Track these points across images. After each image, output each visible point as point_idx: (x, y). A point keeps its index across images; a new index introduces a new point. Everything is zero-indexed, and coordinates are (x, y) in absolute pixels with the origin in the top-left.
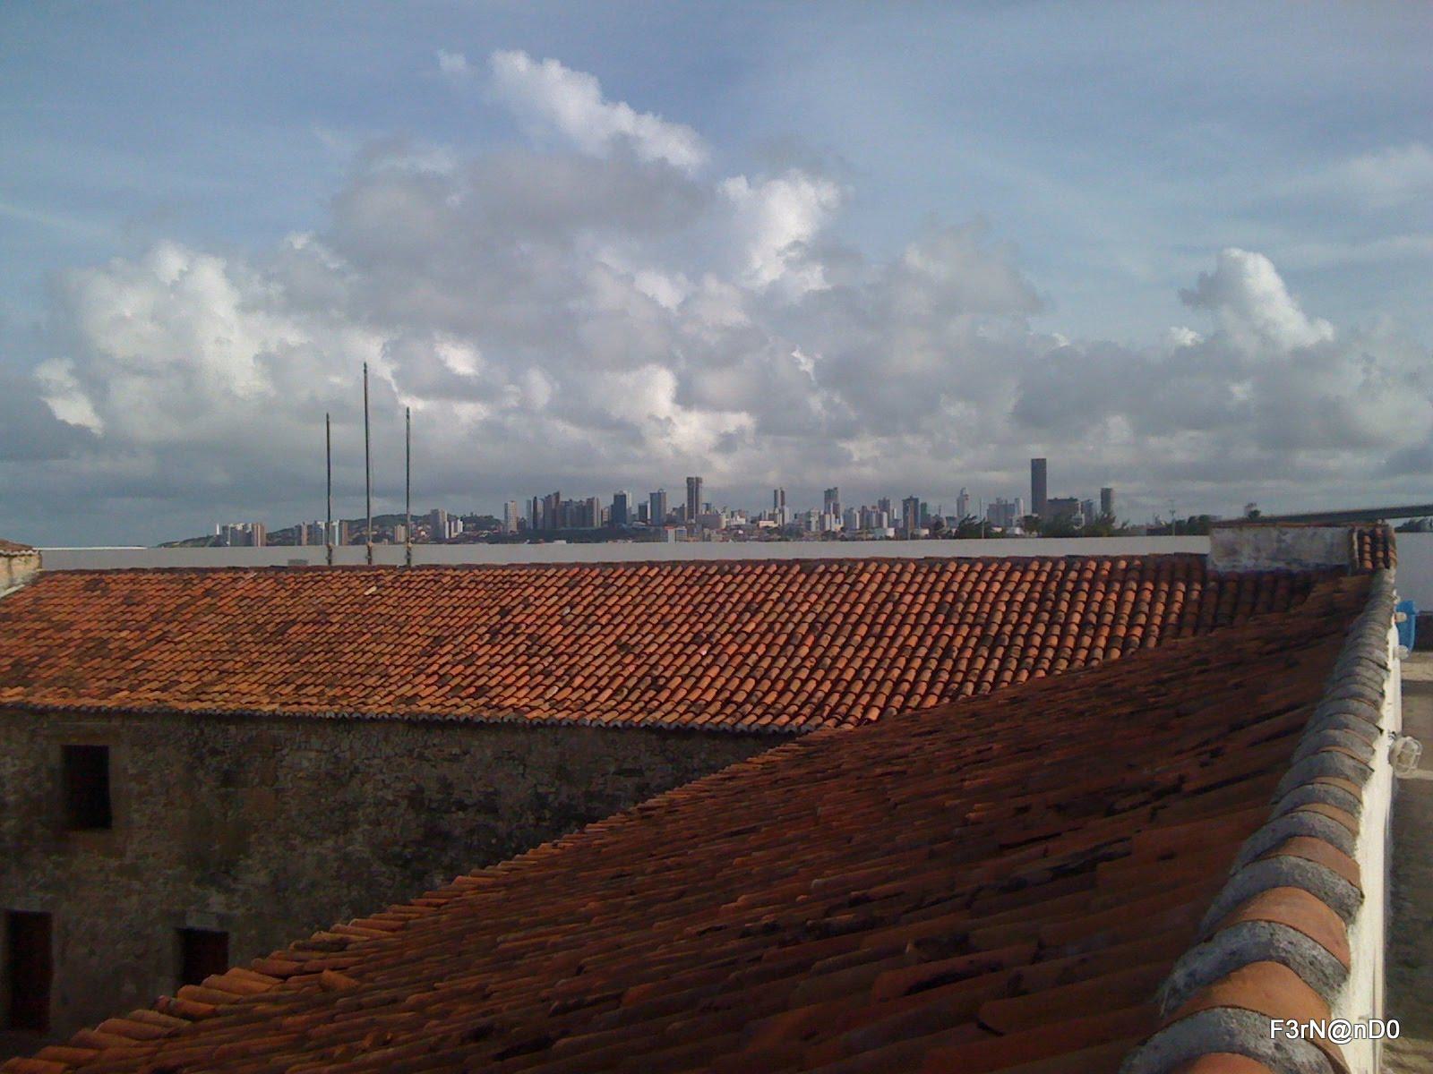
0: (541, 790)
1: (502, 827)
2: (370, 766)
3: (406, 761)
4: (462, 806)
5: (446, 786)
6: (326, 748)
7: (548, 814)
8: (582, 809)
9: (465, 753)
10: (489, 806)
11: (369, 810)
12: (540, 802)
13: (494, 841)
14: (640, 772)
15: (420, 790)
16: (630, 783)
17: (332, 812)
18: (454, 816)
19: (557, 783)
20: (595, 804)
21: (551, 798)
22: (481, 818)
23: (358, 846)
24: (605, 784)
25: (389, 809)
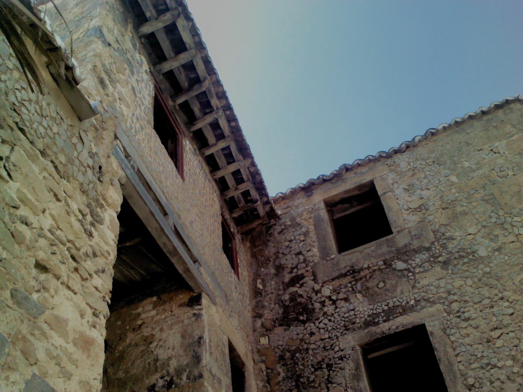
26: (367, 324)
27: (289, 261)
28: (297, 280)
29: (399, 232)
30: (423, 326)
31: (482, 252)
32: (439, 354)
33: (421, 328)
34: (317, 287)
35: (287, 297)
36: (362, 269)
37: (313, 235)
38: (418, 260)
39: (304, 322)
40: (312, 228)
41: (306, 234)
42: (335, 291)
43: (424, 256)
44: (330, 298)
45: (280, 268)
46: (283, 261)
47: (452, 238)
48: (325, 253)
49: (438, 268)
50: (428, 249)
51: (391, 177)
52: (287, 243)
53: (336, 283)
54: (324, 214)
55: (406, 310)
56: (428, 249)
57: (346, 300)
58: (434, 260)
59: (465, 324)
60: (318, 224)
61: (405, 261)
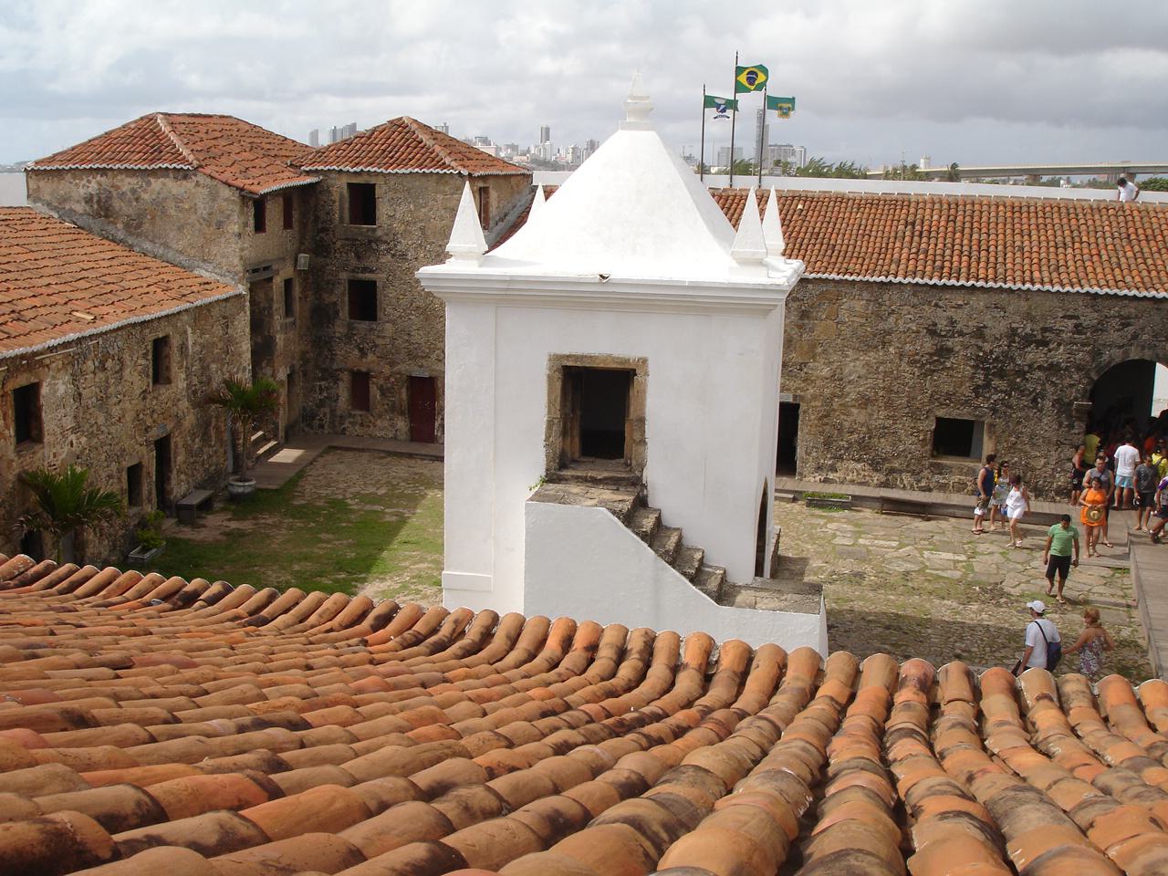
0: (1013, 325)
1: (987, 347)
4: (961, 334)
5: (952, 322)
6: (872, 299)
7: (1017, 339)
8: (1039, 337)
9: (966, 304)
10: (980, 333)
12: (1013, 333)
13: (981, 354)
14: (1077, 318)
15: (935, 325)
16: (1071, 323)
17: (875, 336)
18: (957, 340)
19: (1025, 322)
20: (1047, 334)
21: (1019, 331)
24: (1055, 323)
25: (913, 335)
26: (353, 271)
27: (322, 214)
28: (324, 230)
30: (375, 282)
32: (378, 297)
34: (334, 240)
35: (318, 238)
36: (357, 240)
37: (337, 204)
39: (325, 257)
40: (337, 199)
41: (334, 202)
42: (343, 246)
45: (317, 218)
46: (319, 214)
47: (400, 242)
51: (385, 187)
52: (322, 202)
55: (372, 271)
57: (347, 254)
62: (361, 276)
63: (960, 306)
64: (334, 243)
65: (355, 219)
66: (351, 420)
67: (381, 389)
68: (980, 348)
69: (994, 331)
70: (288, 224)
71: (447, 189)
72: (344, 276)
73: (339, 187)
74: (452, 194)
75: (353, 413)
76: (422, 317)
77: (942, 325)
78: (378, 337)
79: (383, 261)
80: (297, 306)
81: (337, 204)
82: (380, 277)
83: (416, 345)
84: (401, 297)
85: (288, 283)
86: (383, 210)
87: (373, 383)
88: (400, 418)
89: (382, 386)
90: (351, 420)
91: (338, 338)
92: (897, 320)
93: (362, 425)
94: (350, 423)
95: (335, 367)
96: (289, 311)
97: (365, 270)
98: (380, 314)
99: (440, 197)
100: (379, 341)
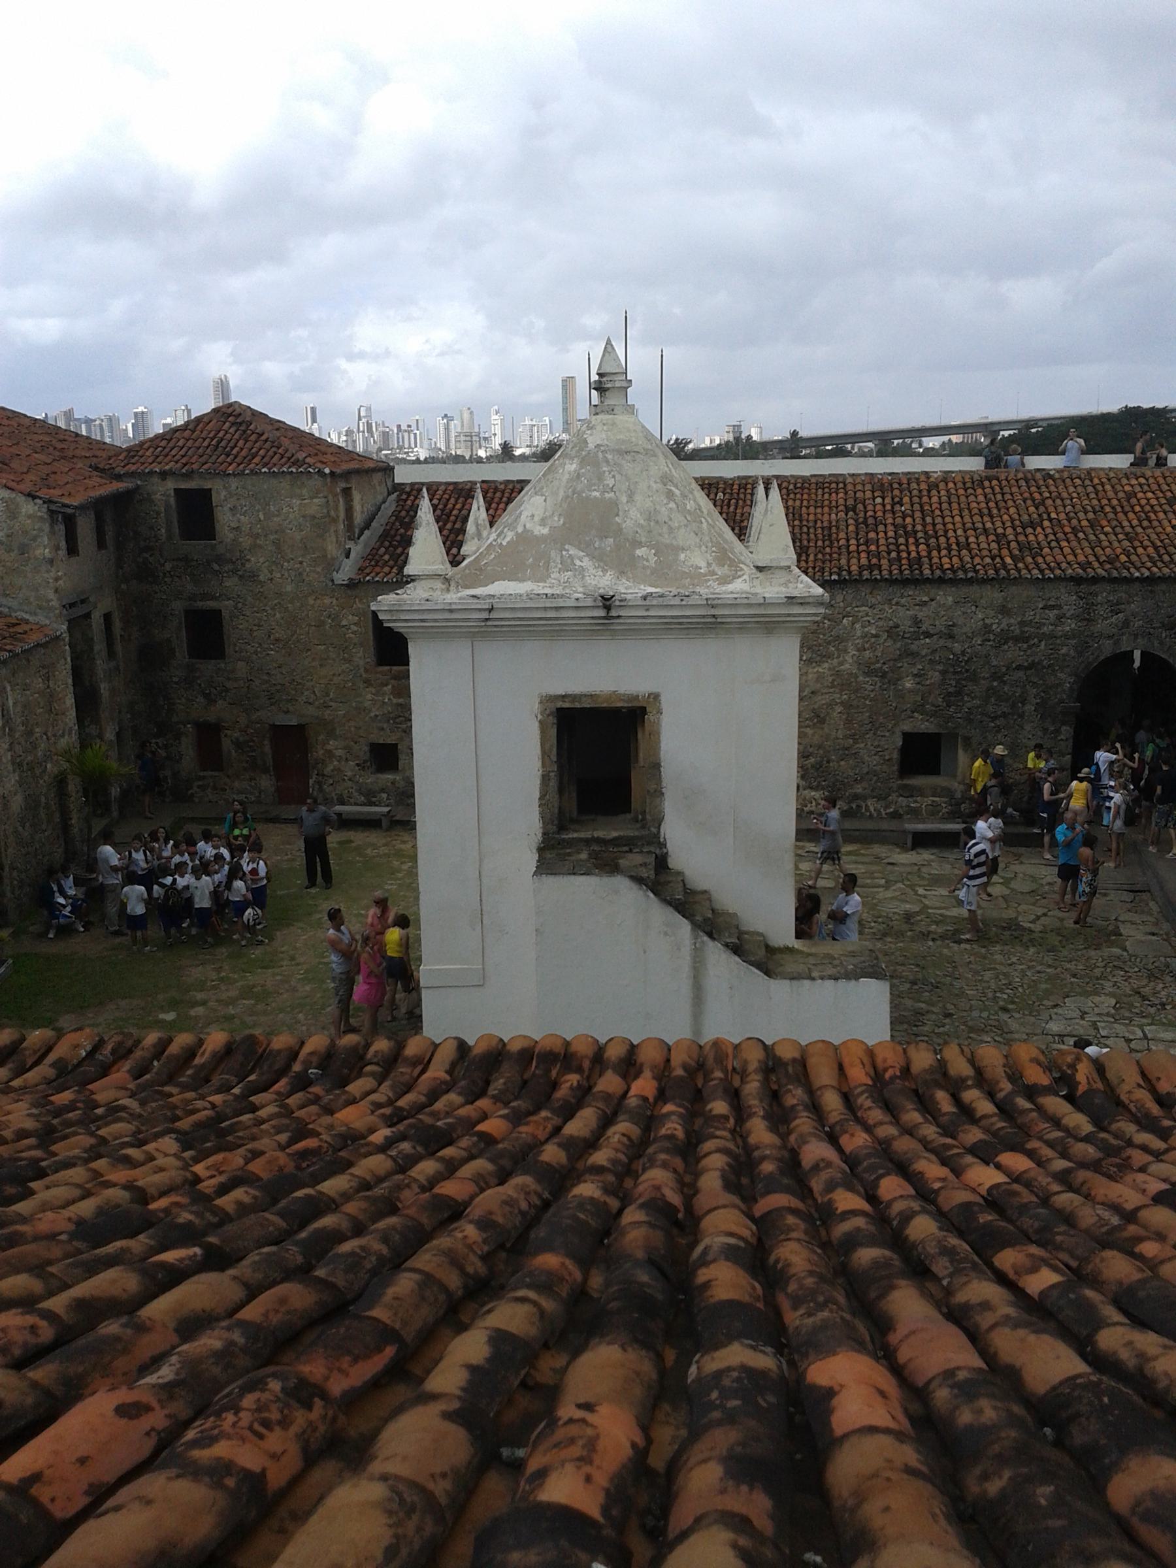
0: (987, 621)
1: (957, 647)
2: (859, 611)
3: (886, 607)
4: (928, 635)
5: (917, 622)
8: (1018, 632)
9: (932, 600)
11: (857, 641)
13: (951, 657)
16: (1052, 614)
18: (923, 642)
19: (1000, 616)
20: (1026, 629)
21: (994, 627)
22: (942, 642)
23: (848, 664)
24: (1035, 615)
25: (873, 640)
29: (221, 542)
31: (261, 578)
33: (217, 614)
35: (141, 560)
37: (162, 515)
38: (226, 568)
41: (158, 513)
43: (230, 566)
44: (169, 572)
47: (248, 560)
48: (170, 537)
49: (236, 579)
50: (234, 563)
51: (224, 493)
53: (175, 563)
54: (172, 501)
55: (214, 598)
56: (234, 563)
57: (179, 577)
58: (234, 572)
59: (241, 617)
60: (168, 506)
61: (219, 565)
62: (199, 604)
63: (925, 604)
64: (163, 565)
65: (189, 533)
66: (200, 783)
67: (238, 745)
68: (950, 650)
69: (964, 630)
70: (101, 544)
71: (304, 491)
72: (178, 606)
73: (163, 491)
74: (312, 498)
75: (202, 774)
76: (283, 651)
77: (906, 626)
78: (229, 679)
79: (227, 584)
80: (119, 648)
81: (162, 515)
82: (226, 606)
83: (279, 687)
84: (255, 628)
85: (107, 617)
86: (225, 519)
87: (226, 736)
88: (264, 776)
89: (237, 739)
90: (200, 783)
91: (176, 683)
92: (853, 624)
93: (215, 788)
94: (199, 787)
95: (175, 719)
96: (111, 654)
97: (205, 596)
98: (229, 650)
99: (296, 502)
100: (229, 685)
